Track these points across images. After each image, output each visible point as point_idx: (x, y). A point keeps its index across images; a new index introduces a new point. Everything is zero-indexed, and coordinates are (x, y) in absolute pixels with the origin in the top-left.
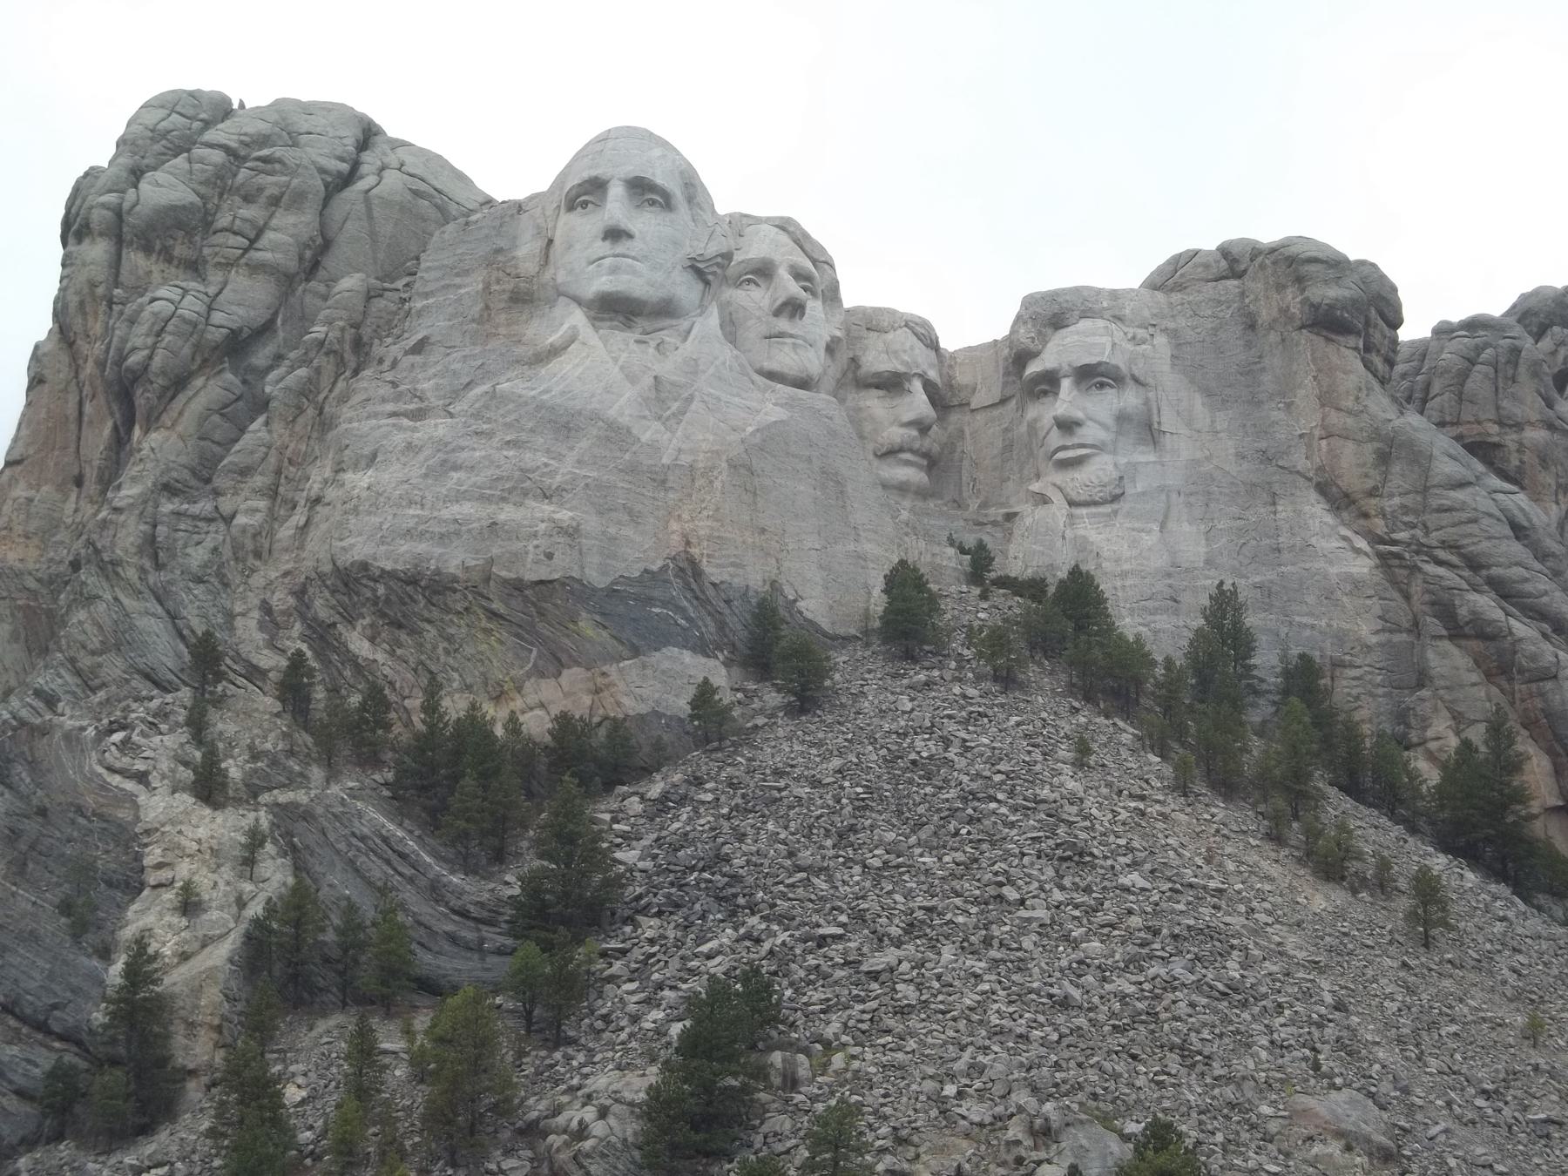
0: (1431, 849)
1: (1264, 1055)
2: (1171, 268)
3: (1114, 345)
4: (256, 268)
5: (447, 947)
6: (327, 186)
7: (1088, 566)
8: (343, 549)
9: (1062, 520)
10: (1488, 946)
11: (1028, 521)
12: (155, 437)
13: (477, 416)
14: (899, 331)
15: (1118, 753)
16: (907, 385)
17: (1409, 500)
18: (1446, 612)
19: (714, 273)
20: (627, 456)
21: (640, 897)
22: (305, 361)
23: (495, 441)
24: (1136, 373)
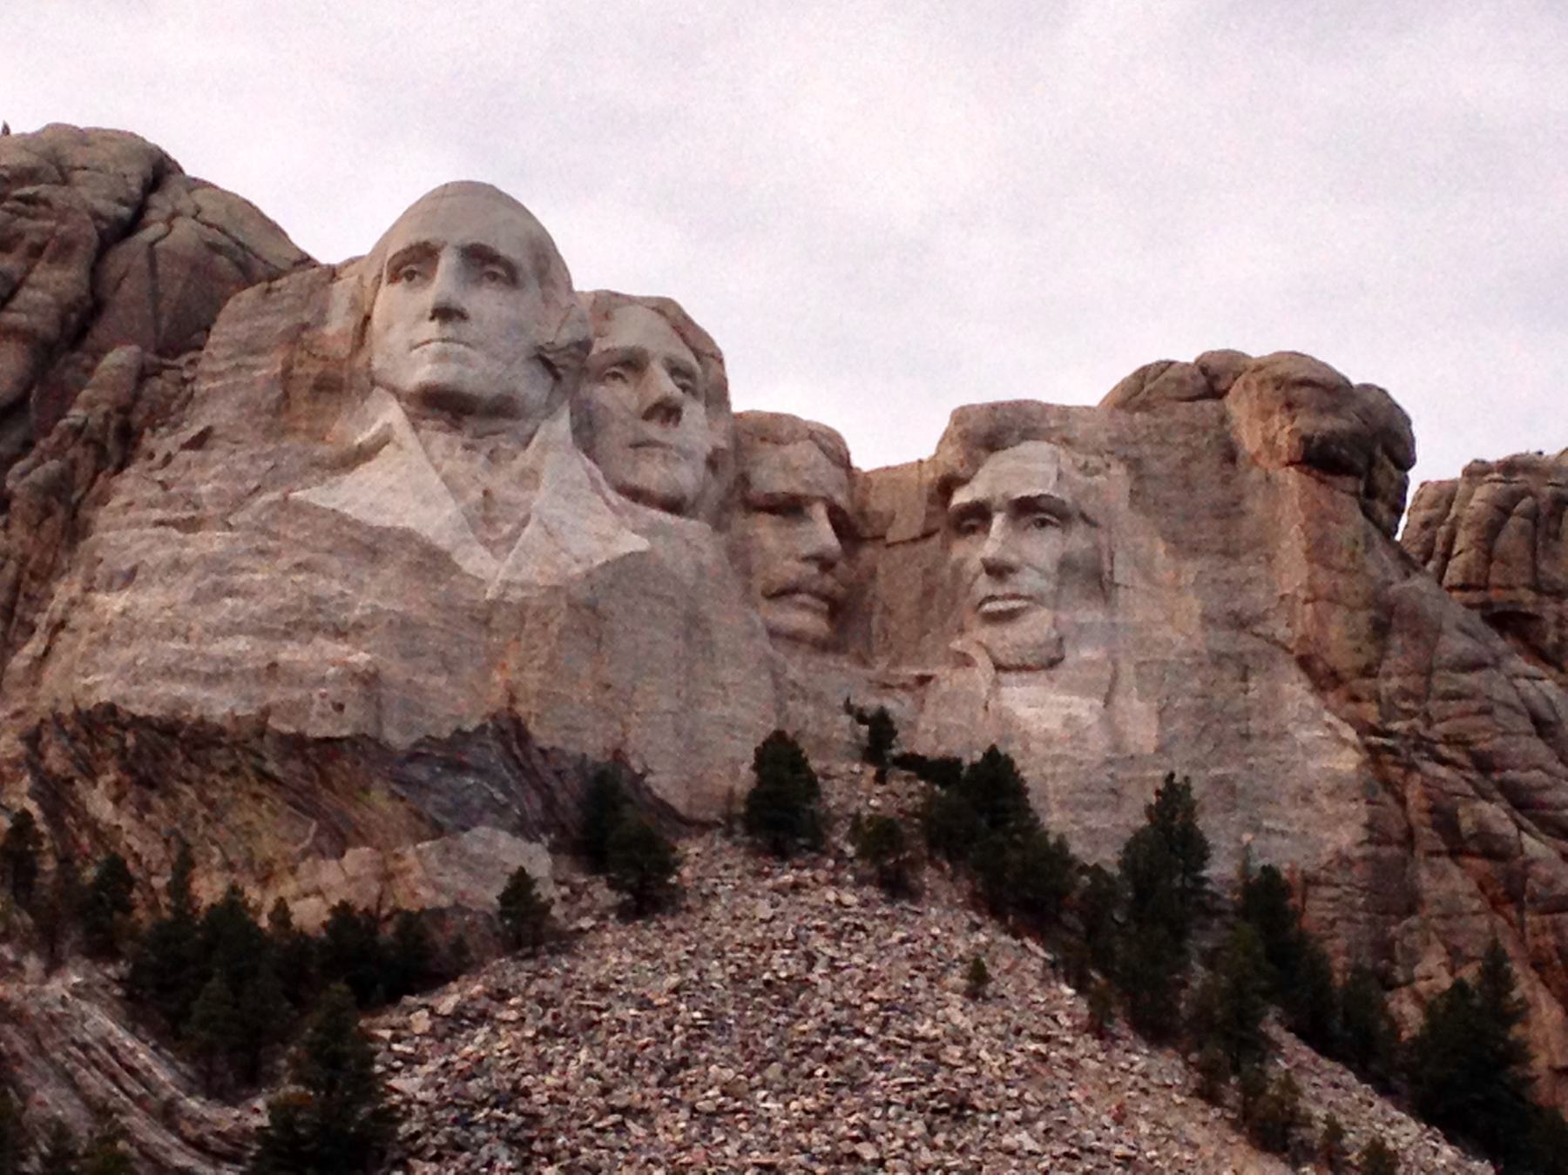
3: (1060, 476)
6: (102, 234)
7: (1013, 749)
8: (88, 688)
11: (945, 686)
13: (263, 530)
15: (1023, 983)
16: (807, 510)
17: (1411, 683)
18: (1445, 821)
19: (564, 367)
20: (443, 588)
21: (417, 1135)
22: (57, 451)
23: (284, 562)
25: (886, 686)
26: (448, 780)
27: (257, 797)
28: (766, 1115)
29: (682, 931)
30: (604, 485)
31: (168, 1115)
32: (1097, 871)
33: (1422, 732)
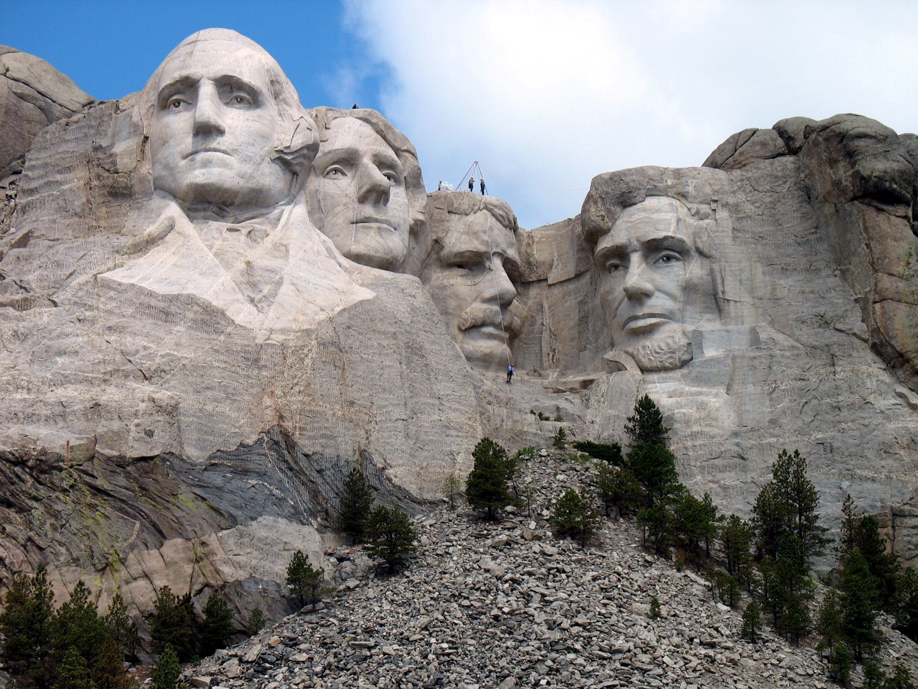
2: (731, 147)
3: (679, 220)
11: (604, 387)
14: (479, 214)
16: (488, 264)
19: (301, 164)
20: (222, 338)
24: (700, 245)
25: (558, 391)
26: (237, 483)
27: (92, 507)
29: (426, 582)
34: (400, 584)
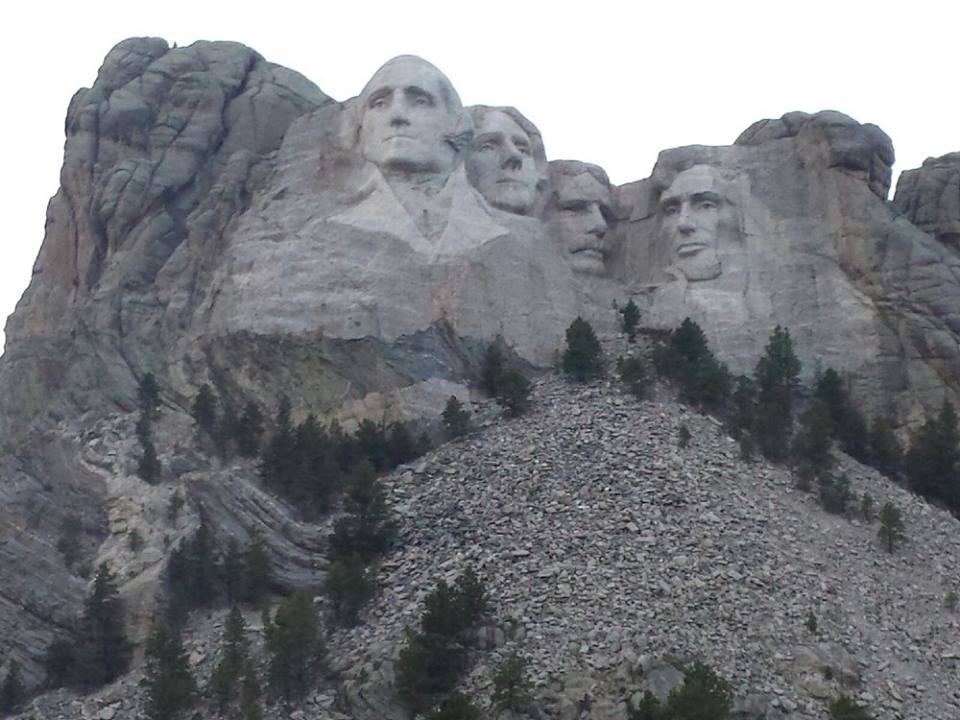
0: (903, 491)
1: (780, 622)
3: (715, 181)
4: (182, 148)
5: (294, 567)
7: (699, 321)
8: (234, 323)
9: (683, 291)
10: (931, 551)
12: (119, 256)
15: (708, 438)
16: (589, 208)
18: (919, 341)
19: (461, 145)
20: (407, 261)
27: (320, 372)
28: (581, 512)
29: (536, 423)
30: (485, 203)
31: (285, 531)
32: (742, 378)
33: (906, 298)
34: (519, 425)
